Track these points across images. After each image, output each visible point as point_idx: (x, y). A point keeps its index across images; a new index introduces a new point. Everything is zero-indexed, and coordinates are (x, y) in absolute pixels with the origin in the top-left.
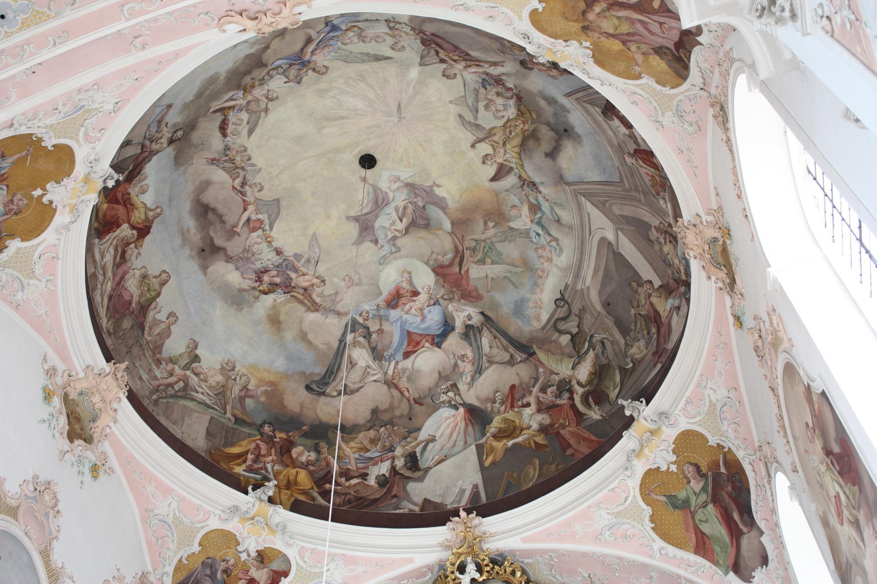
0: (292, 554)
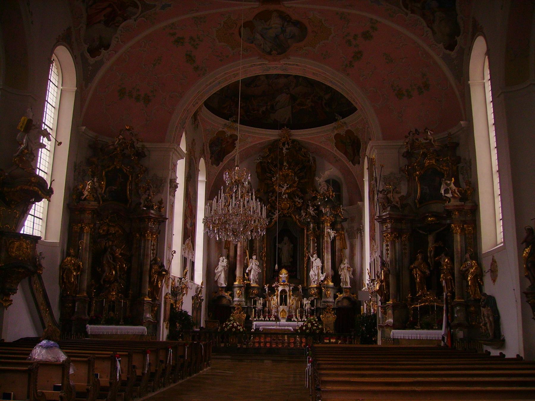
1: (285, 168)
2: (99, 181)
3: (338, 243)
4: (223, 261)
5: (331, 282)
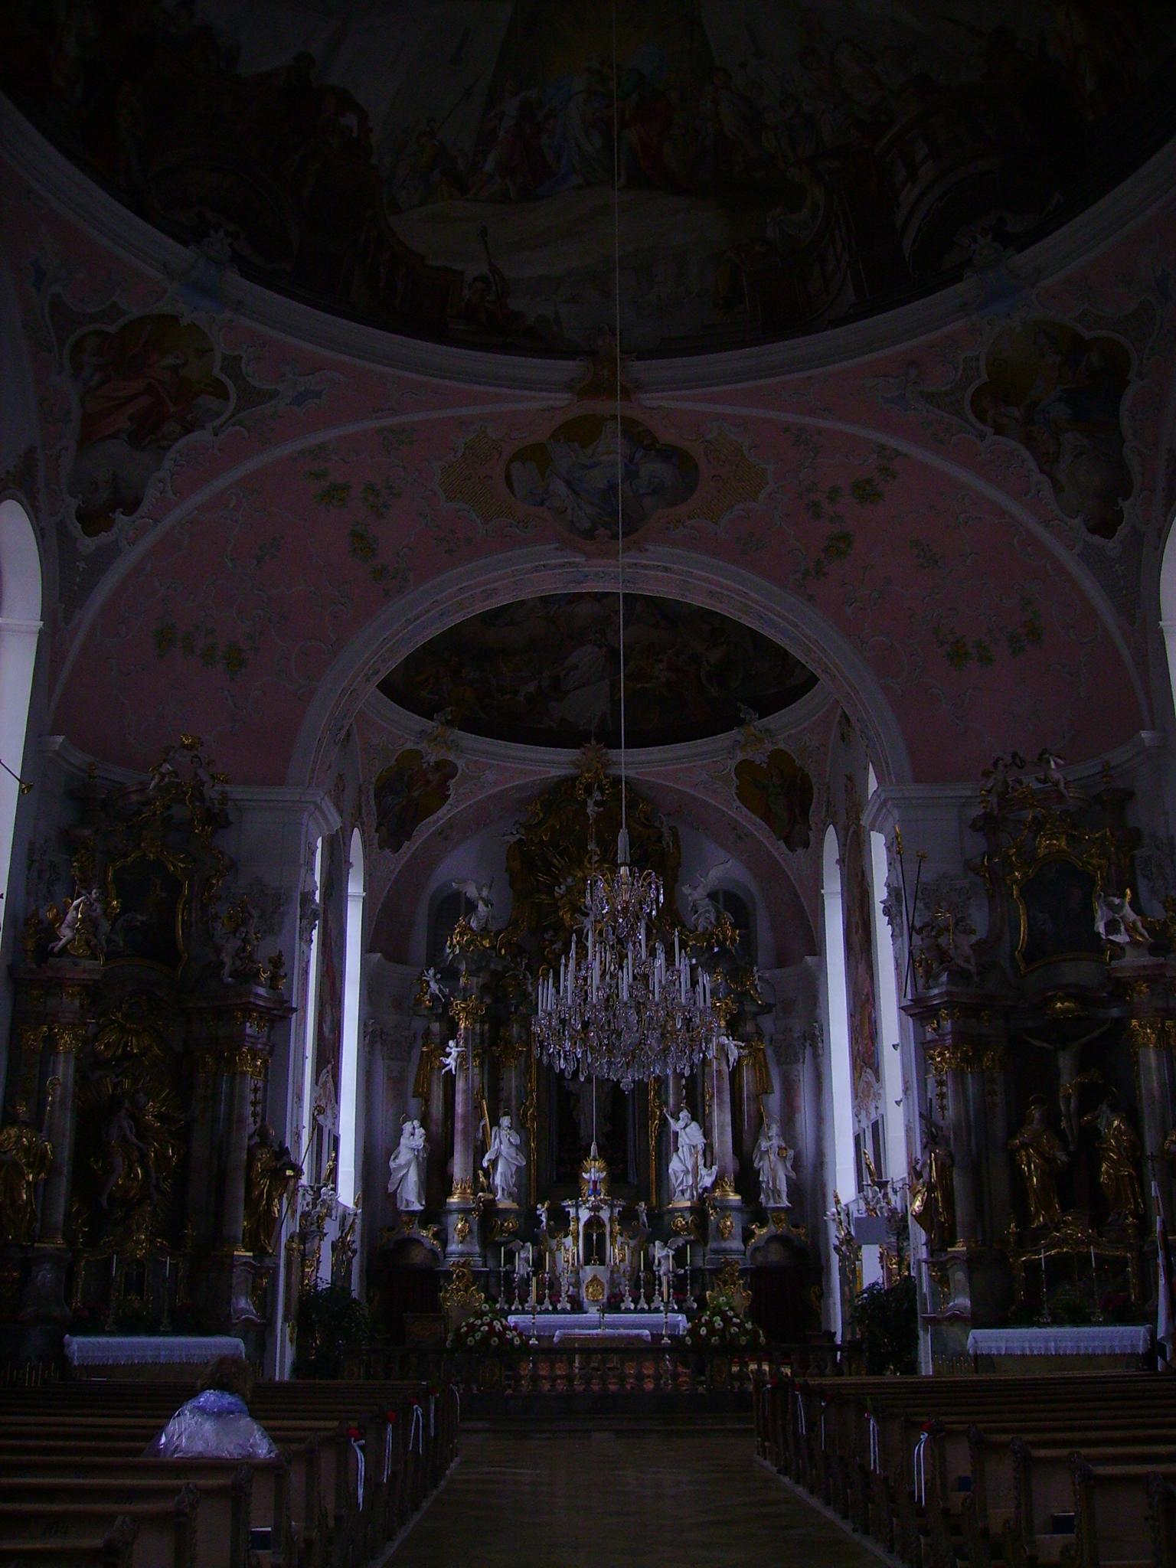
0: (460, 763)
1: (591, 858)
2: (105, 896)
3: (747, 1076)
4: (413, 1134)
5: (732, 1192)
